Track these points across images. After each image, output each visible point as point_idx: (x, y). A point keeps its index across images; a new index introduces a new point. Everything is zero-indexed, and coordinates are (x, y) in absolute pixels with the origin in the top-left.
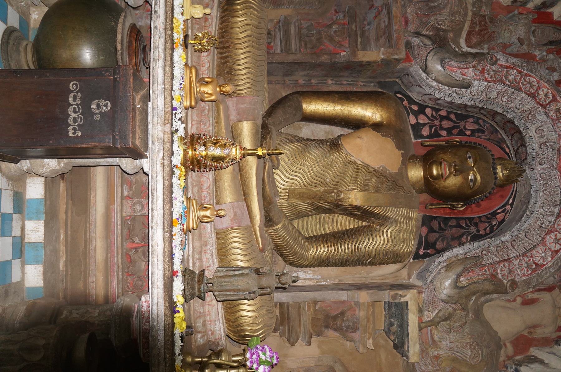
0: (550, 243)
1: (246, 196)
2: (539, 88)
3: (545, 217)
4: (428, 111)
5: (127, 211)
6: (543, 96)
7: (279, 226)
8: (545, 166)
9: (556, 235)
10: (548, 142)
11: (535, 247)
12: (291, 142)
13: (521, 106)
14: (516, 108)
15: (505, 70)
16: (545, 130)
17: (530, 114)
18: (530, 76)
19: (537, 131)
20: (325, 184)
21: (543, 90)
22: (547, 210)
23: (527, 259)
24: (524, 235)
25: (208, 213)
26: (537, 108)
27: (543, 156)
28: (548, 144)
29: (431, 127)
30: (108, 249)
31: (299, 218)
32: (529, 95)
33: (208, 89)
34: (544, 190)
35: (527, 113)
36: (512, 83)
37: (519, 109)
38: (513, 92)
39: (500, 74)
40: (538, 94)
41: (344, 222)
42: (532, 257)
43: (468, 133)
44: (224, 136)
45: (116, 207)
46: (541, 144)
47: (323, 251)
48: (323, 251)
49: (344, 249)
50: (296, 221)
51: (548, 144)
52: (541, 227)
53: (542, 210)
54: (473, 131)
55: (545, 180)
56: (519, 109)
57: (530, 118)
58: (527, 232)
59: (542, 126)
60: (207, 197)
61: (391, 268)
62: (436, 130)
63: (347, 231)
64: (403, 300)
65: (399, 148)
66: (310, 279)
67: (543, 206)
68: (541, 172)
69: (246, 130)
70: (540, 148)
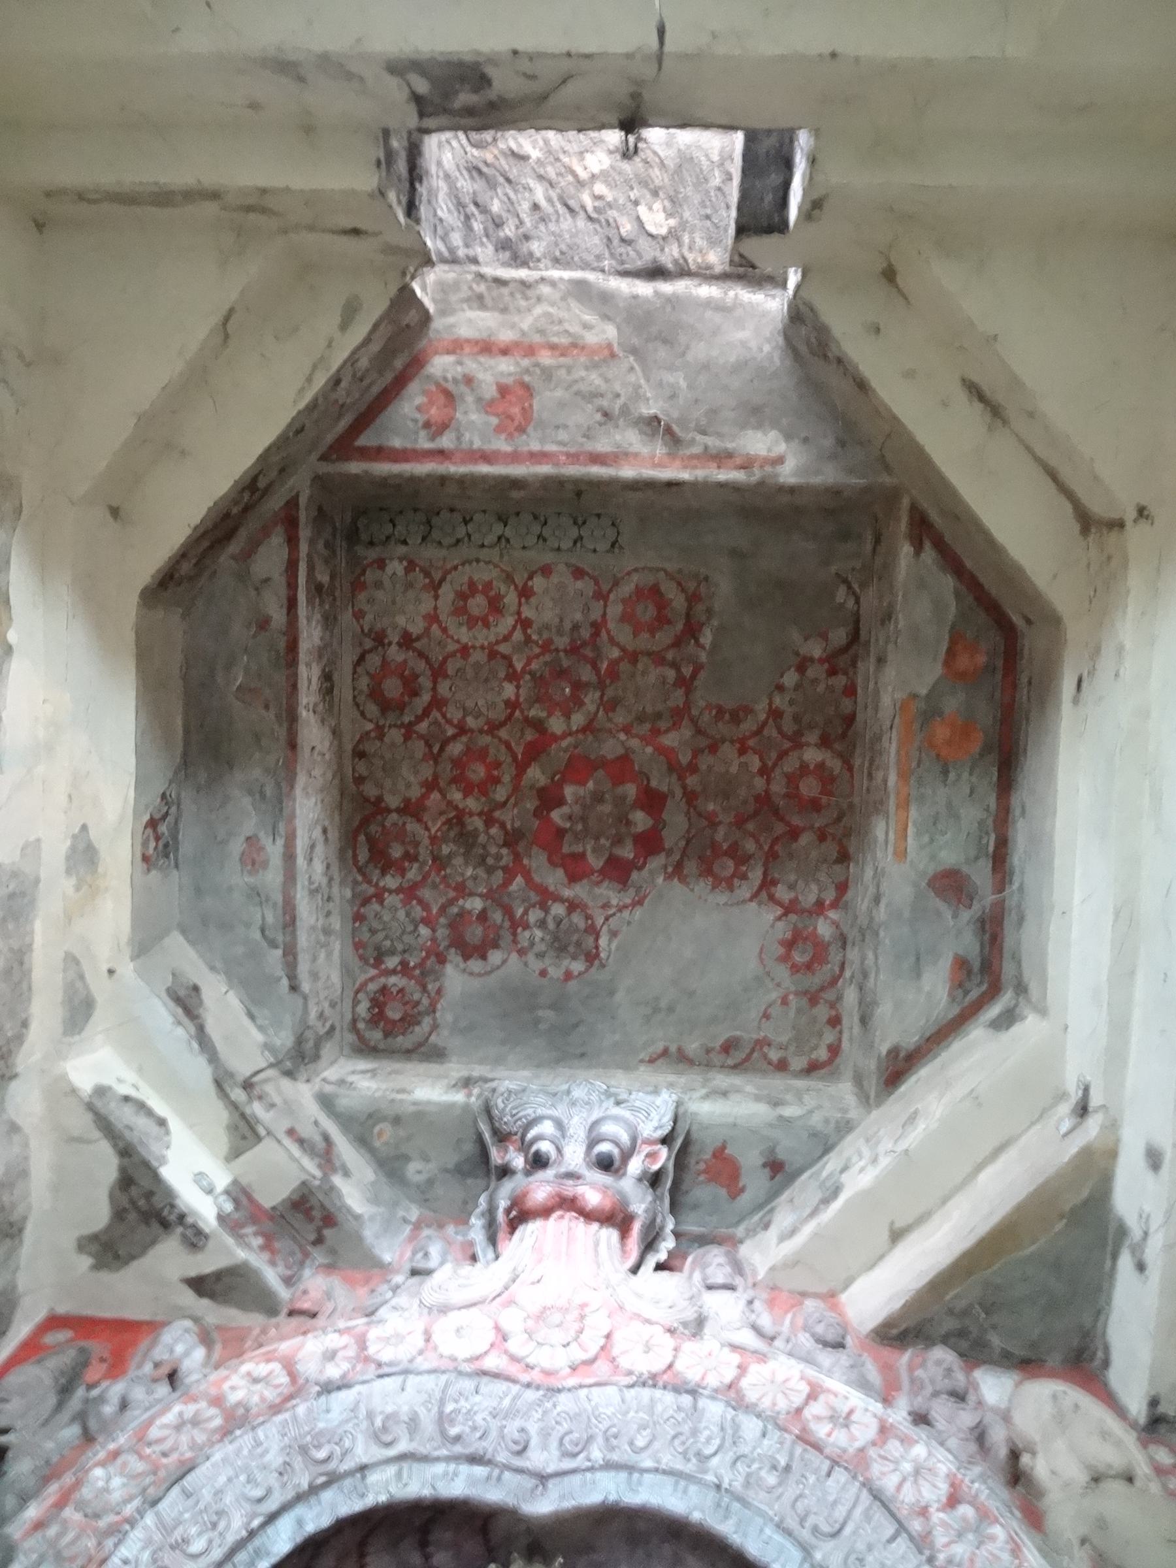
0: (853, 1438)
2: (217, 1401)
3: (744, 1449)
6: (259, 1387)
8: (533, 1429)
9: (818, 1418)
10: (442, 1402)
11: (877, 1496)
13: (259, 1477)
14: (260, 1500)
15: (69, 1512)
16: (389, 1409)
17: (304, 1450)
18: (150, 1423)
19: (388, 1438)
21: (233, 1388)
22: (716, 1442)
23: (940, 1539)
24: (830, 1545)
26: (295, 1418)
27: (494, 1434)
28: (449, 1408)
32: (226, 1433)
34: (631, 1444)
35: (298, 1462)
36: (144, 1490)
37: (269, 1491)
38: (187, 1495)
39: (70, 1536)
40: (239, 1404)
42: (924, 1512)
46: (443, 1433)
51: (449, 1408)
52: (788, 1468)
53: (715, 1461)
55: (590, 1439)
56: (269, 1491)
57: (321, 1454)
58: (815, 1530)
59: (370, 1416)
67: (698, 1454)
68: (556, 1453)
70: (457, 1439)
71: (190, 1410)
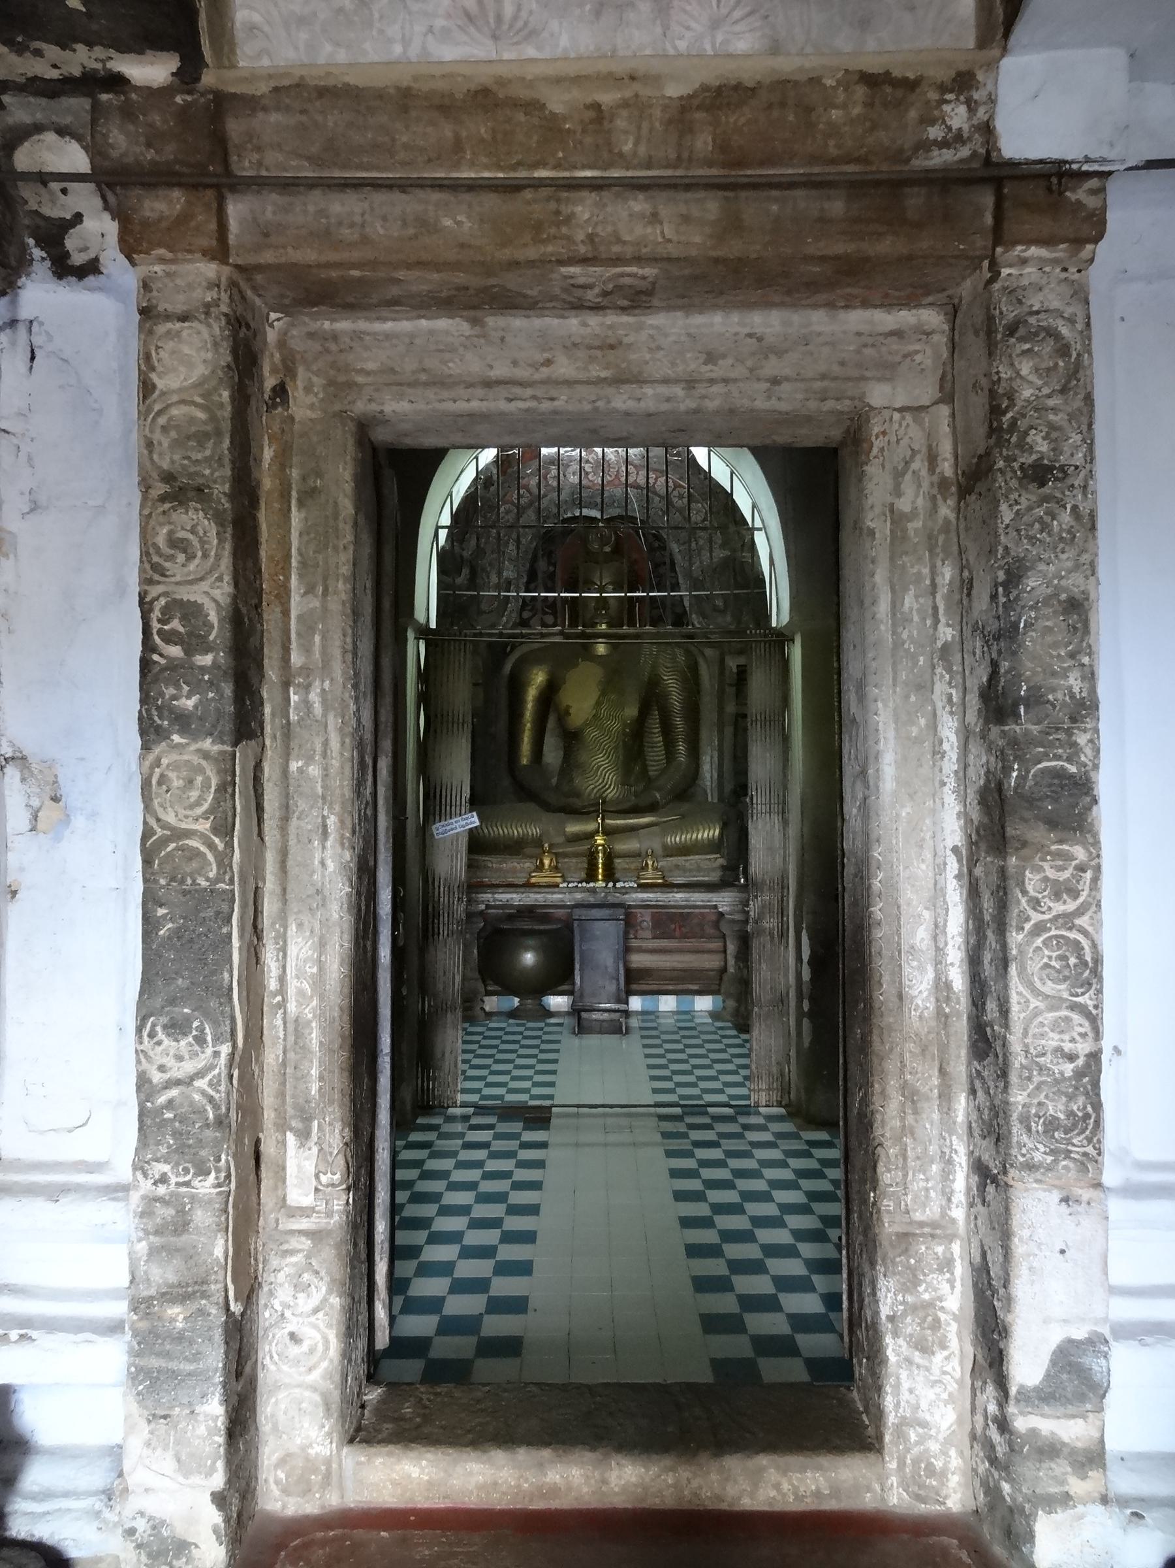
1: (633, 829)
4: (526, 615)
5: (648, 934)
7: (658, 796)
12: (571, 780)
20: (616, 748)
25: (650, 863)
29: (545, 613)
30: (681, 951)
31: (647, 771)
33: (547, 862)
41: (654, 724)
43: (552, 569)
44: (584, 847)
45: (644, 944)
47: (681, 747)
48: (681, 747)
49: (678, 722)
50: (651, 773)
54: (549, 563)
60: (634, 864)
61: (704, 671)
62: (547, 607)
63: (660, 719)
64: (735, 670)
65: (577, 665)
66: (712, 757)
69: (573, 828)
71: (507, 506)
